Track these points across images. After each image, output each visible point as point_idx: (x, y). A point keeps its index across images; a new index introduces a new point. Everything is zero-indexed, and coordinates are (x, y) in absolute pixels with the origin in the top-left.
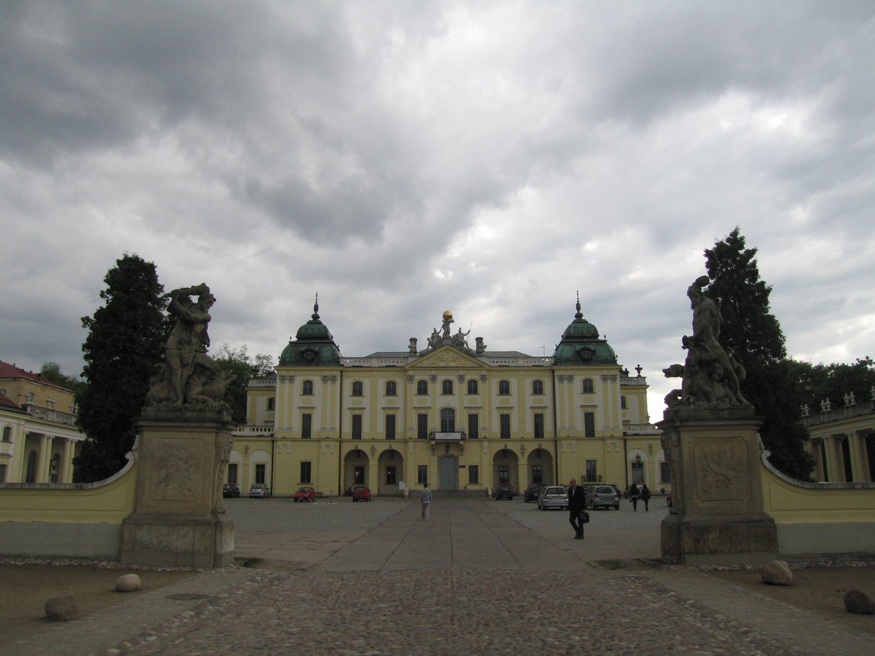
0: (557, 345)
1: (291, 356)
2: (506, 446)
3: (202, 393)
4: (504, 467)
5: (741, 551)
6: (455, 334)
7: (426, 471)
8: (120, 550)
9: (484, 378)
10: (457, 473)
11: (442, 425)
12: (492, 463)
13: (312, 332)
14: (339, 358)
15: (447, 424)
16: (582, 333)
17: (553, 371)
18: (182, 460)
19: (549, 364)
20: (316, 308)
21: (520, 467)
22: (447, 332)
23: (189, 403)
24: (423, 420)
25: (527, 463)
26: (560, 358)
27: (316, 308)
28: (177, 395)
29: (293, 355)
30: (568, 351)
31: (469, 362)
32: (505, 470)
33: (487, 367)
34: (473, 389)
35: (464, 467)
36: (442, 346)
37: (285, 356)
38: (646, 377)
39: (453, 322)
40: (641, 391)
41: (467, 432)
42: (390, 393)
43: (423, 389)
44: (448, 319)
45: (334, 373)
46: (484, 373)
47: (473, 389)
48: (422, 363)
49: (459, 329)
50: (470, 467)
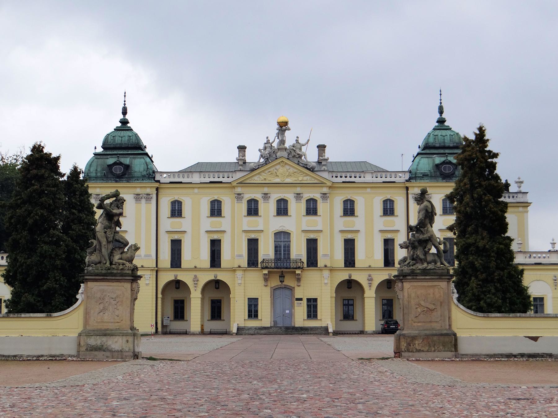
0: (415, 156)
1: (96, 170)
2: (350, 276)
3: (121, 259)
4: (348, 300)
5: (434, 351)
6: (292, 144)
7: (256, 306)
8: (78, 352)
9: (324, 196)
10: (292, 307)
11: (276, 251)
12: (334, 295)
13: (121, 140)
14: (154, 172)
15: (281, 250)
16: (444, 142)
17: (407, 188)
18: (113, 298)
19: (403, 180)
20: (125, 112)
21: (367, 301)
22: (282, 142)
23: (114, 265)
24: (253, 244)
25: (374, 295)
26: (416, 173)
27: (125, 112)
28: (105, 259)
29: (99, 169)
30: (426, 164)
31: (308, 178)
32: (350, 303)
33: (329, 184)
35: (301, 299)
36: (276, 159)
37: (89, 170)
38: (528, 193)
39: (289, 129)
40: (521, 209)
41: (305, 260)
42: (214, 214)
44: (283, 126)
45: (148, 191)
46: (325, 190)
48: (253, 178)
49: (296, 139)
50: (309, 300)
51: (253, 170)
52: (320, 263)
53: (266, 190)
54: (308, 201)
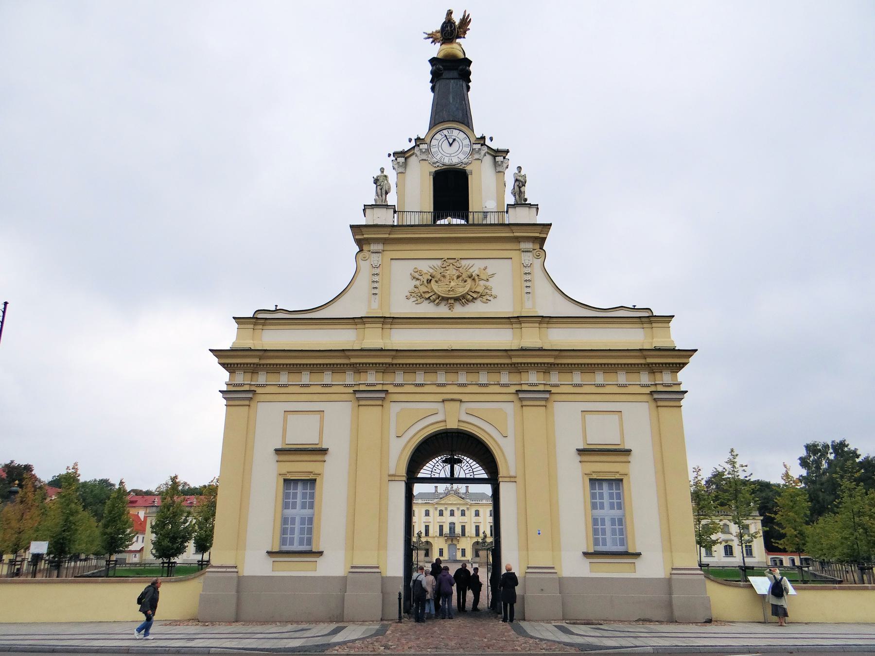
7: (442, 552)
9: (468, 509)
10: (456, 552)
24: (441, 527)
33: (470, 504)
34: (463, 514)
41: (461, 534)
43: (441, 514)
46: (468, 506)
47: (463, 514)
50: (462, 549)
51: (441, 498)
52: (466, 535)
53: (446, 506)
54: (462, 510)
